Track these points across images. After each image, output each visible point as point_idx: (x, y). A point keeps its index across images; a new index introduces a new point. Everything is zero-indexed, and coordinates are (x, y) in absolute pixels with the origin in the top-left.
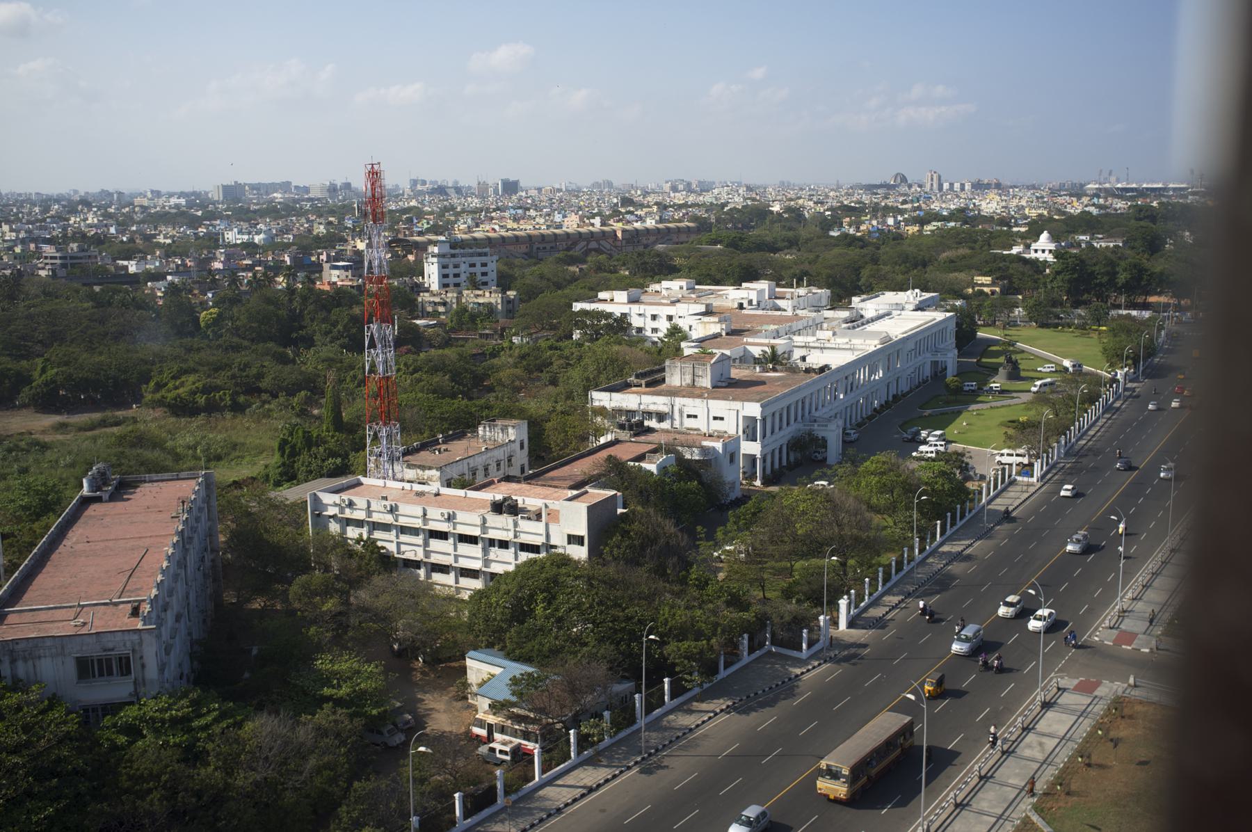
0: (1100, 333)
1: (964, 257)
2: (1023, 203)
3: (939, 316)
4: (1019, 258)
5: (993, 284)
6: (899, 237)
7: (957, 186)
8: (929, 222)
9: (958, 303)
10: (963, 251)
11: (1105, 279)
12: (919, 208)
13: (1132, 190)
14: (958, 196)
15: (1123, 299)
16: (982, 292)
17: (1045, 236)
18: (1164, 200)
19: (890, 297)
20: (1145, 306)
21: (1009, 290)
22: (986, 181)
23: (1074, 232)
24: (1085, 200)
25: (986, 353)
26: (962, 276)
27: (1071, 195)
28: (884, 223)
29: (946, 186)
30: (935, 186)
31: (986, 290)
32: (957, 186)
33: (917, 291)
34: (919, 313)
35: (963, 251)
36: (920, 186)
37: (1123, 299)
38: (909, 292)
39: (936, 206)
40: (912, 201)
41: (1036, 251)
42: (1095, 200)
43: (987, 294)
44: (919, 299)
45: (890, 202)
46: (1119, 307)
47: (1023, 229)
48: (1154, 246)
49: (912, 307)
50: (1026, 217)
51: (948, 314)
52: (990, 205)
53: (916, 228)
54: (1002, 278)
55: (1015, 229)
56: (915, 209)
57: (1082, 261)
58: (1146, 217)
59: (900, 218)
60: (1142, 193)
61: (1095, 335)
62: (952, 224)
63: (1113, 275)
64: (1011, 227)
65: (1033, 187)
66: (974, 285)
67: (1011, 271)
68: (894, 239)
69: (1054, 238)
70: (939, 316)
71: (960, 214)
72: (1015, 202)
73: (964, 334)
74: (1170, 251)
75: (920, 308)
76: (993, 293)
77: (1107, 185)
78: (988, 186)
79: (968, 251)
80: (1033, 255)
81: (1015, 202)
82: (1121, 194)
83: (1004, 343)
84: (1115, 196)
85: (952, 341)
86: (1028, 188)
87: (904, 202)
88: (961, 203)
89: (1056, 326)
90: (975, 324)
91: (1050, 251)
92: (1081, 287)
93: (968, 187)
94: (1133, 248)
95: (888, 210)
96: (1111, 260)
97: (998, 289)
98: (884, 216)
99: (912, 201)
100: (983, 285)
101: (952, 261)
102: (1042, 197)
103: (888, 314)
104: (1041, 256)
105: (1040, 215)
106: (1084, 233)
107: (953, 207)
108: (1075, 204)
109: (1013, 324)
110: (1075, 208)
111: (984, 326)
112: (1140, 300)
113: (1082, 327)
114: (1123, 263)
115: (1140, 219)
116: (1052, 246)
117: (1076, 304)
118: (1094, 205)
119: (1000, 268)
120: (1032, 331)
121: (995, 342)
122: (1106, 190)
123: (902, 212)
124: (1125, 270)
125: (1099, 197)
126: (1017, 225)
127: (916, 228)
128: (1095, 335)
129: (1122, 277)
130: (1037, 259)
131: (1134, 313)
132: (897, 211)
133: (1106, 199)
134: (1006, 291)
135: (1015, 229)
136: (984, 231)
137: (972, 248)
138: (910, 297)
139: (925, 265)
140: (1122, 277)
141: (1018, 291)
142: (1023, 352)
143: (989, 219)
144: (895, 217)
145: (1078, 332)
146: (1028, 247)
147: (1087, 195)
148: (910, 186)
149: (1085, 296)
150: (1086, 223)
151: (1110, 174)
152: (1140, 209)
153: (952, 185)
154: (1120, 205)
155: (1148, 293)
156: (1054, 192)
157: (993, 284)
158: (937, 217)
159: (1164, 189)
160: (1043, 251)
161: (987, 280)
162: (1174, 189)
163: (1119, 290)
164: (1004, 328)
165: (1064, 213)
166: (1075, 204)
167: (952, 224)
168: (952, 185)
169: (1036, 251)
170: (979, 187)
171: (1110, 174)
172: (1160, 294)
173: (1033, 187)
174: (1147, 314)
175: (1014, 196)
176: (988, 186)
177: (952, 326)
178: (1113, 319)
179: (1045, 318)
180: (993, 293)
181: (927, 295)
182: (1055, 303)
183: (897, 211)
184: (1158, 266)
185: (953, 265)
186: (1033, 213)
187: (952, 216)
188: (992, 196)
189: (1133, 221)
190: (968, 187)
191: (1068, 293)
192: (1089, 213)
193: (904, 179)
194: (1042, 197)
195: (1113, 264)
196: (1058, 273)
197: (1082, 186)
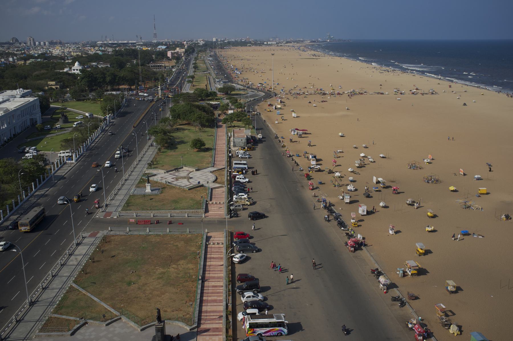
0: (101, 101)
1: (43, 74)
2: (71, 50)
3: (31, 99)
4: (67, 73)
5: (56, 84)
6: (13, 66)
7: (42, 43)
8: (29, 59)
9: (40, 93)
10: (43, 71)
11: (102, 80)
12: (24, 53)
13: (115, 44)
14: (43, 48)
15: (109, 88)
16: (52, 89)
17: (77, 64)
18: (127, 47)
19: (9, 93)
20: (118, 90)
21: (63, 87)
22: (55, 41)
23: (89, 62)
24: (96, 48)
25: (55, 113)
26: (42, 82)
27: (91, 47)
28: (8, 60)
29: (37, 43)
30: (32, 43)
31: (53, 87)
32: (42, 43)
33: (21, 89)
34: (22, 99)
35: (43, 71)
36: (25, 43)
37: (109, 88)
38: (18, 90)
39: (32, 52)
40: (21, 50)
41: (74, 70)
42: (101, 48)
43: (54, 89)
44: (22, 92)
45: (10, 51)
46: (108, 91)
47: (70, 61)
48: (121, 66)
49: (19, 96)
50: (72, 56)
51: (35, 98)
52: (56, 51)
53: (23, 62)
54: (60, 82)
55: (67, 61)
56: (22, 54)
57: (92, 73)
58: (119, 55)
59: (15, 58)
60: (119, 45)
61: (99, 102)
62: (39, 60)
63: (104, 78)
64: (65, 60)
65: (76, 43)
66: (48, 85)
67: (64, 79)
68: (12, 67)
69: (80, 64)
70: (31, 99)
71: (43, 56)
72: (66, 50)
73: (44, 106)
74: (129, 68)
75: (23, 96)
76: (57, 88)
77: (105, 42)
78: (56, 43)
79: (45, 71)
80: (73, 72)
81: (68, 49)
82: (111, 45)
83: (61, 109)
84: (109, 46)
85: (38, 110)
86: (74, 44)
87: (17, 51)
88: (44, 51)
89: (84, 100)
90: (48, 101)
91: (80, 70)
92: (93, 83)
93: (47, 43)
94: (113, 67)
95: (8, 55)
96: (103, 72)
97: (58, 87)
98: (8, 57)
99: (21, 50)
100: (52, 85)
101: (38, 76)
102: (79, 48)
103: (8, 100)
104: (76, 72)
105: (77, 55)
106: (95, 62)
107: (40, 52)
108: (92, 50)
109: (66, 101)
110: (92, 51)
111: (54, 102)
112: (117, 87)
113: (94, 100)
114: (108, 73)
115: (117, 56)
116: (80, 68)
117: (92, 91)
118: (100, 50)
119: (58, 78)
120: (74, 103)
121: (58, 108)
122: (105, 44)
123: (16, 55)
124: (109, 76)
125: (102, 47)
126: (68, 60)
127: (23, 62)
128: (99, 102)
129: (108, 79)
130: (74, 73)
131: (114, 93)
132: (13, 55)
133: (105, 48)
134: (62, 87)
135: (67, 61)
136: (53, 63)
137: (47, 70)
138: (19, 92)
139: (26, 78)
140: (108, 79)
141: (67, 87)
142: (70, 111)
143: (56, 57)
144: (13, 58)
145: (92, 102)
146: (71, 68)
147: (97, 46)
148: (20, 44)
149: (94, 88)
150: (96, 58)
151: (106, 37)
152: (116, 51)
153: (40, 43)
154: (110, 50)
155: (119, 84)
156: (84, 45)
157: (56, 84)
158: (32, 57)
159: (128, 43)
160: (77, 70)
161: (53, 83)
162: (131, 43)
163: (107, 84)
164: (62, 102)
165: (88, 54)
166: (92, 50)
167: (39, 60)
168: (40, 43)
169: (74, 70)
170: (52, 44)
171: (106, 37)
172: (123, 84)
173: (76, 43)
174: (118, 93)
175: (67, 47)
176: (56, 43)
177: (38, 103)
178: (106, 95)
179: (80, 96)
180: (57, 88)
181: (26, 91)
182: (83, 91)
183: (13, 55)
184: (122, 73)
185: (39, 77)
186: (75, 54)
187: (39, 56)
188: (57, 47)
189: (115, 57)
190: (47, 43)
191: (88, 86)
192: (98, 54)
193: (17, 40)
194: (79, 48)
195: (104, 74)
196: (83, 78)
197: (96, 42)
